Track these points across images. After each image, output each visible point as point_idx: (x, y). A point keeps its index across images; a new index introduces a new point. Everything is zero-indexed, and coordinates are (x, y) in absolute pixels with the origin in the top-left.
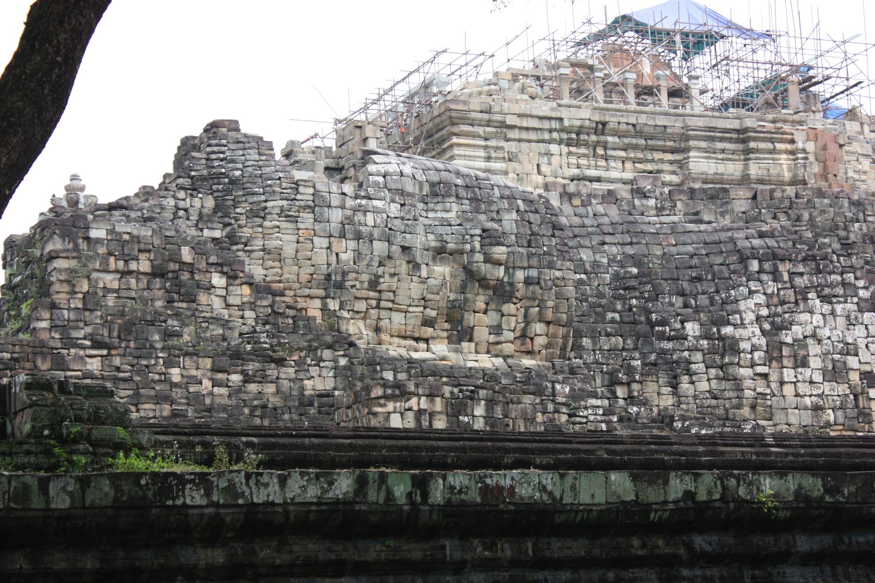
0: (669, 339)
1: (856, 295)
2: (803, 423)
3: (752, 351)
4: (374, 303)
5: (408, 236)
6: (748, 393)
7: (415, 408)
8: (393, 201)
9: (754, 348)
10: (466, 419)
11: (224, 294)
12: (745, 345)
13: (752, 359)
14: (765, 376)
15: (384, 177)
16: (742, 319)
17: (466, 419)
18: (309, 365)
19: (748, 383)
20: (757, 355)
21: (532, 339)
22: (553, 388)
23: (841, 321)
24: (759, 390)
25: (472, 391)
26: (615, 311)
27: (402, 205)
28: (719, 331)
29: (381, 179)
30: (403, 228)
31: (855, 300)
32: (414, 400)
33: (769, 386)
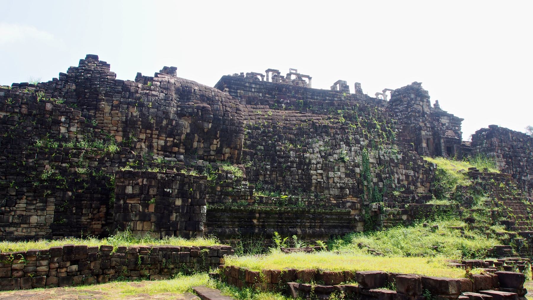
0: (282, 158)
1: (359, 143)
2: (336, 194)
3: (316, 164)
4: (149, 135)
5: (167, 107)
6: (314, 181)
7: (141, 184)
8: (162, 92)
9: (318, 163)
10: (168, 190)
11: (68, 126)
12: (314, 161)
13: (316, 167)
14: (321, 174)
15: (160, 83)
16: (313, 151)
17: (168, 190)
18: (107, 161)
19: (314, 177)
20: (318, 166)
21: (224, 155)
22: (227, 175)
23: (353, 153)
24: (318, 180)
25: (173, 177)
26: (262, 145)
27: (166, 94)
28: (303, 155)
29: (158, 84)
30: (164, 104)
31: (359, 145)
32: (140, 180)
33: (322, 179)
